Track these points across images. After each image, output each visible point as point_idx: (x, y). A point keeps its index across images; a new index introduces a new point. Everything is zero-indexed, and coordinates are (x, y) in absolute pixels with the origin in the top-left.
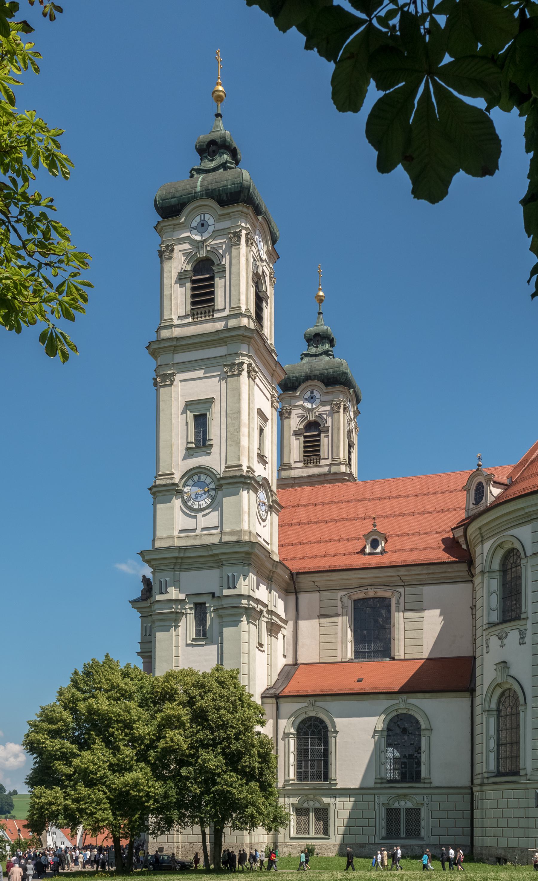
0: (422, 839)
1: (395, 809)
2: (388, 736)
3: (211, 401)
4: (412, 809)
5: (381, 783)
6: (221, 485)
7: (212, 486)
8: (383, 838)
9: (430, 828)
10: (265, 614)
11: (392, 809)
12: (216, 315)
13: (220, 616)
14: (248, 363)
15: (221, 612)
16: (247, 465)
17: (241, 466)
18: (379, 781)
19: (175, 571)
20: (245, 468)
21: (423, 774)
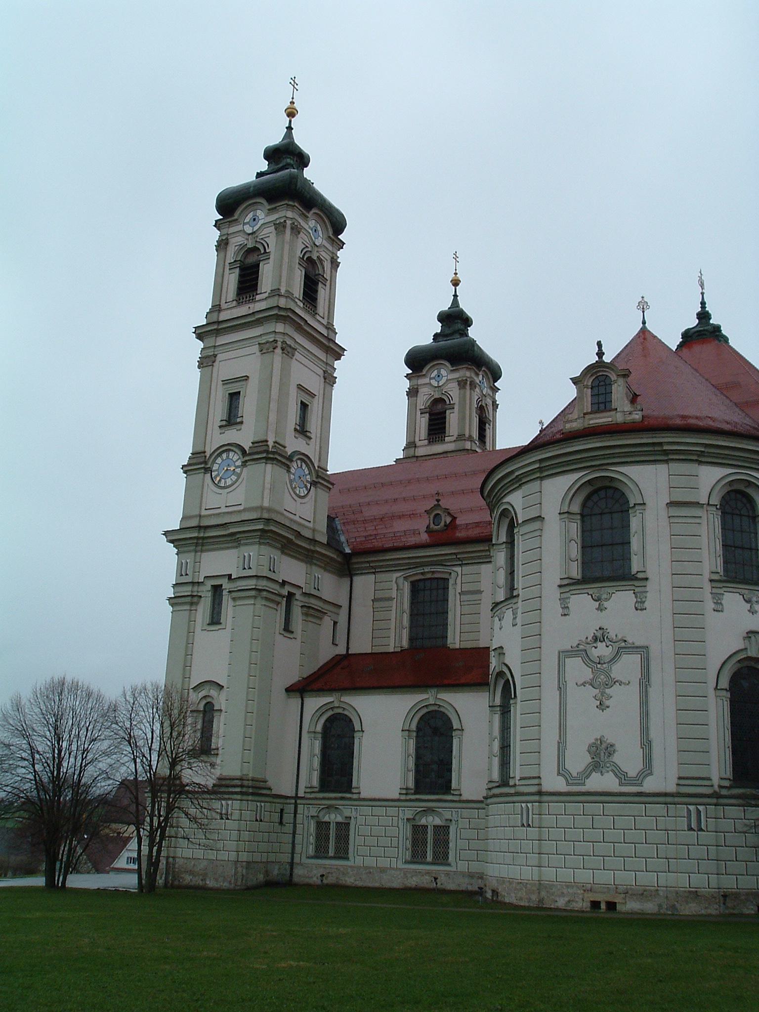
0: (449, 865)
1: (422, 826)
2: (417, 737)
3: (246, 378)
4: (441, 827)
5: (406, 794)
6: (246, 461)
7: (239, 463)
8: (406, 862)
9: (458, 852)
10: (298, 597)
11: (419, 826)
12: (258, 297)
13: (234, 599)
14: (282, 340)
15: (234, 595)
16: (274, 440)
17: (267, 441)
18: (404, 792)
19: (196, 552)
20: (271, 444)
21: (454, 785)
